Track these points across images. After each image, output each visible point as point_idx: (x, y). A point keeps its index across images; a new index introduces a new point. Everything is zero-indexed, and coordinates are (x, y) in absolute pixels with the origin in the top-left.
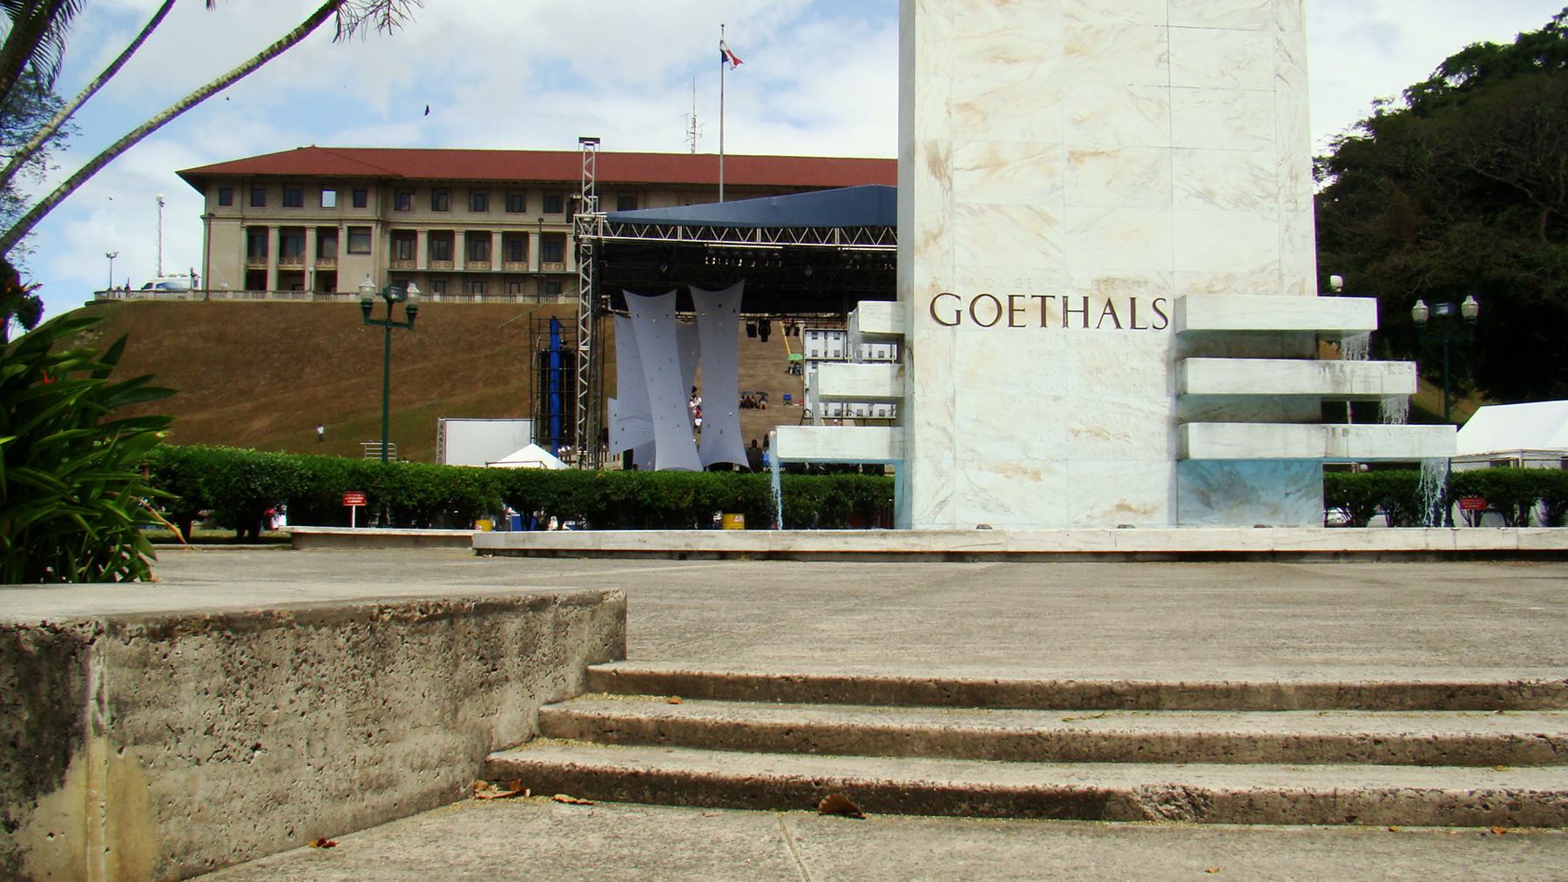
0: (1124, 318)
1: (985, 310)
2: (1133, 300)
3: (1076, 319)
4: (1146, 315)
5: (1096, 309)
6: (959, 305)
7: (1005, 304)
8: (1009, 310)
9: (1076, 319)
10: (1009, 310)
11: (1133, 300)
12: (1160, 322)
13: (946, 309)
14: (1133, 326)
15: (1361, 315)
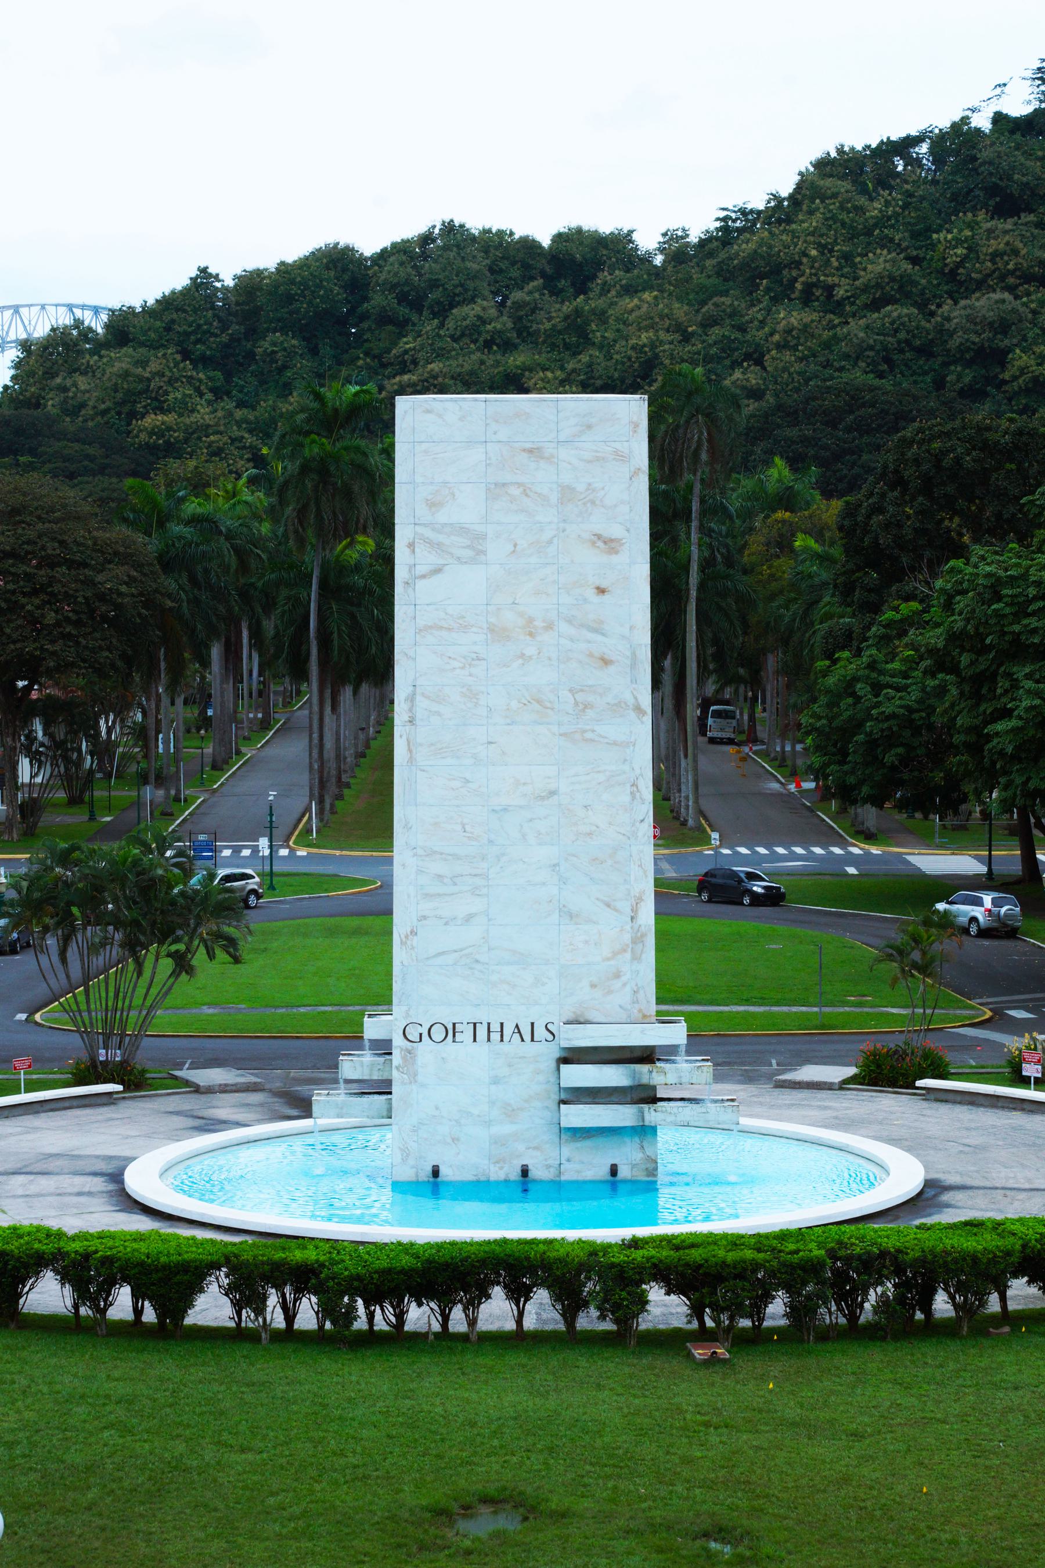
0: (527, 1037)
1: (438, 1033)
2: (532, 1024)
3: (495, 1037)
4: (540, 1033)
5: (508, 1031)
6: (420, 1030)
7: (450, 1027)
8: (452, 1031)
9: (495, 1037)
10: (452, 1031)
11: (532, 1024)
12: (550, 1037)
13: (413, 1035)
14: (532, 1040)
15: (676, 1034)
